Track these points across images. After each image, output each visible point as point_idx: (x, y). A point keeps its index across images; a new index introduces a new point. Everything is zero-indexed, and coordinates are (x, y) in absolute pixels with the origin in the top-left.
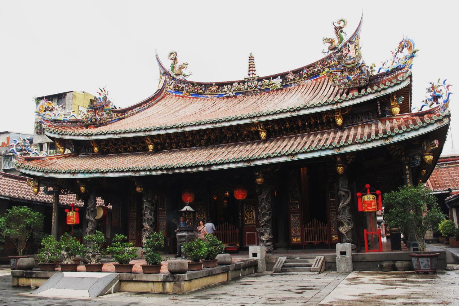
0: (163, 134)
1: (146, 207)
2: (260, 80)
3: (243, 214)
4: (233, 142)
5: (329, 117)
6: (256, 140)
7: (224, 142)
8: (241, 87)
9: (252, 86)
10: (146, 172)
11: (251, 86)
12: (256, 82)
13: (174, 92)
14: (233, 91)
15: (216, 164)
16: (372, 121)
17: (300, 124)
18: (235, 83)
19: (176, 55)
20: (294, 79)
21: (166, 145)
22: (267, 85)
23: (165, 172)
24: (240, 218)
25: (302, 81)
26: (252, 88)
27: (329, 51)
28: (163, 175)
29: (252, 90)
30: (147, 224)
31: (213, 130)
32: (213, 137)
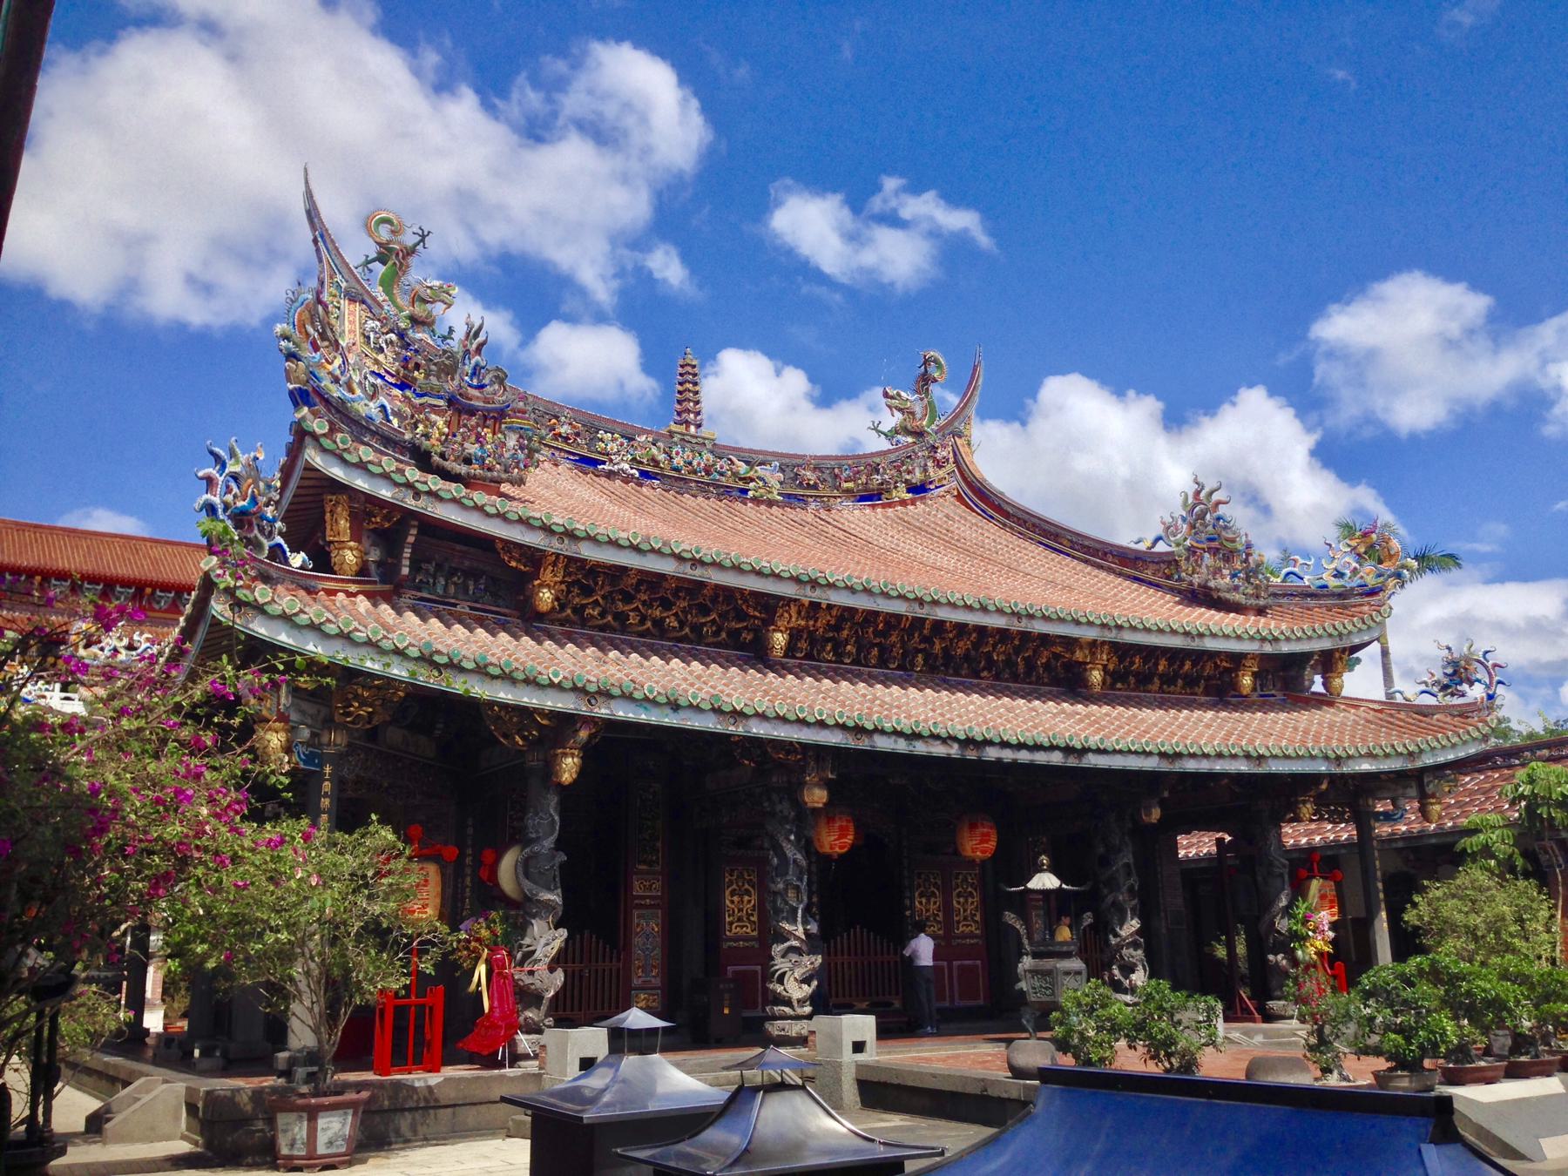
0: (830, 607)
1: (795, 861)
2: (719, 451)
3: (912, 900)
4: (988, 679)
5: (1217, 667)
6: (1044, 684)
7: (963, 672)
8: (661, 457)
9: (695, 463)
10: (896, 742)
11: (690, 463)
12: (711, 457)
13: (395, 385)
14: (634, 460)
15: (1100, 751)
16: (1273, 696)
17: (1161, 668)
18: (643, 438)
19: (423, 240)
20: (815, 487)
21: (803, 645)
22: (741, 479)
23: (954, 751)
24: (908, 913)
25: (835, 497)
26: (695, 472)
27: (896, 431)
28: (947, 760)
29: (693, 477)
30: (801, 928)
31: (1003, 634)
32: (962, 647)
